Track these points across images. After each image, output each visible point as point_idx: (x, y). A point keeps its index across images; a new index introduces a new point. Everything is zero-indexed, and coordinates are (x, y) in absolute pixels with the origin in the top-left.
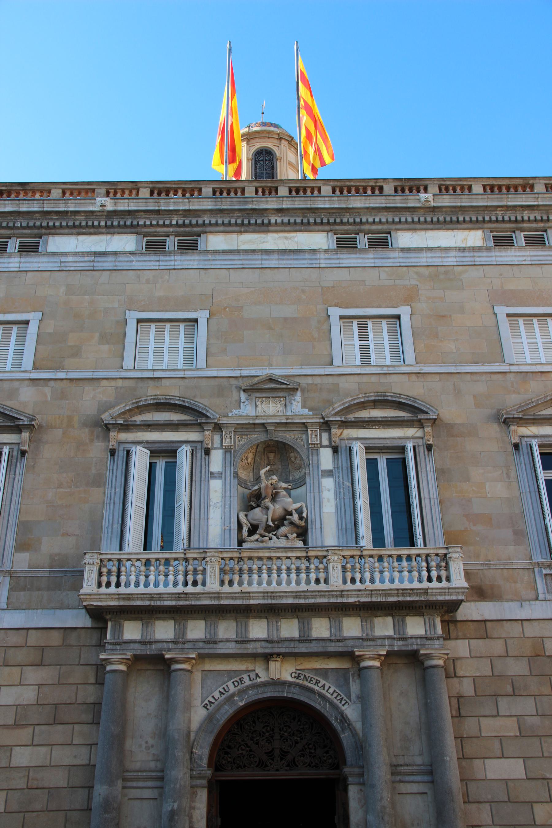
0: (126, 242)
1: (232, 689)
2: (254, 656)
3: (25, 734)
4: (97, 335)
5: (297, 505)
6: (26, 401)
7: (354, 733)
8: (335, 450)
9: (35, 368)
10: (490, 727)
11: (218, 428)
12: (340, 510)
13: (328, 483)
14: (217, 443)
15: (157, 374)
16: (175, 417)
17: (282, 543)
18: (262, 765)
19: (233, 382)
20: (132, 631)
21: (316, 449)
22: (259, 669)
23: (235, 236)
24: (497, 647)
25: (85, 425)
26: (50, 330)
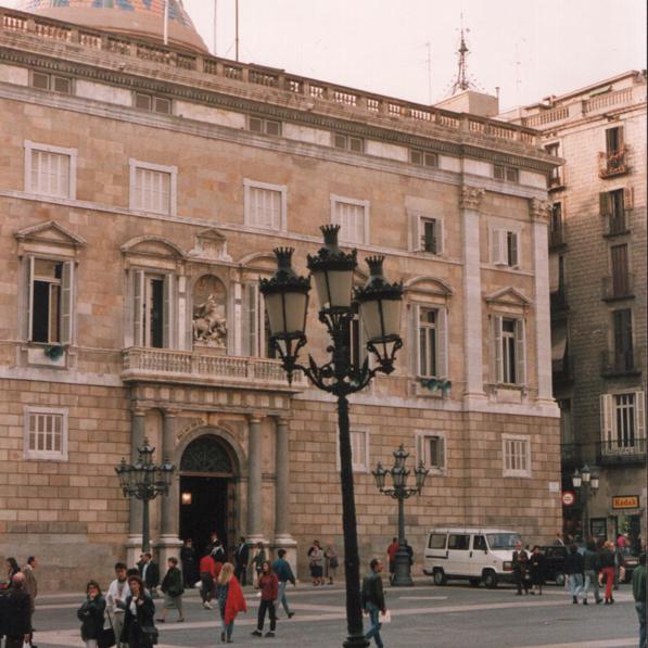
0: (124, 97)
1: (191, 429)
2: (202, 412)
3: (93, 447)
4: (112, 176)
5: (223, 320)
6: (74, 223)
7: (244, 456)
8: (243, 286)
9: (78, 198)
10: (301, 456)
11: (184, 262)
12: (243, 328)
13: (238, 308)
14: (182, 273)
15: (149, 216)
16: (164, 252)
17: (212, 344)
18: (198, 469)
19: (191, 228)
20: (149, 393)
21: (233, 283)
22: (204, 418)
23: (192, 105)
24: (308, 415)
25: (110, 248)
26: (83, 166)
